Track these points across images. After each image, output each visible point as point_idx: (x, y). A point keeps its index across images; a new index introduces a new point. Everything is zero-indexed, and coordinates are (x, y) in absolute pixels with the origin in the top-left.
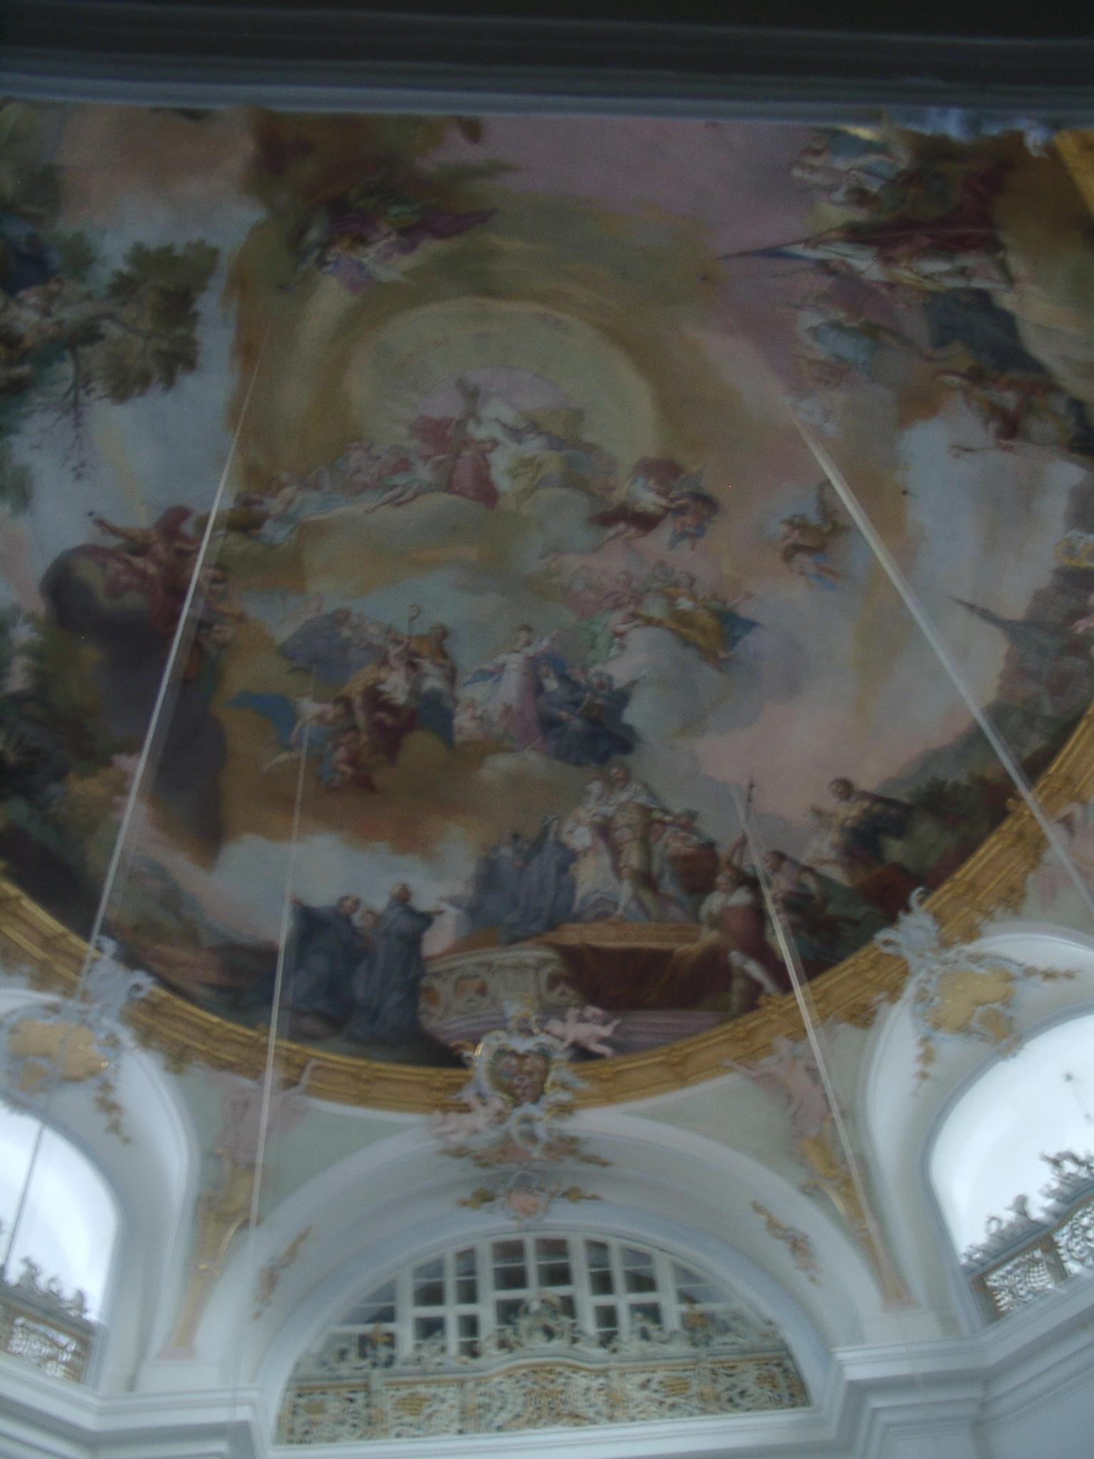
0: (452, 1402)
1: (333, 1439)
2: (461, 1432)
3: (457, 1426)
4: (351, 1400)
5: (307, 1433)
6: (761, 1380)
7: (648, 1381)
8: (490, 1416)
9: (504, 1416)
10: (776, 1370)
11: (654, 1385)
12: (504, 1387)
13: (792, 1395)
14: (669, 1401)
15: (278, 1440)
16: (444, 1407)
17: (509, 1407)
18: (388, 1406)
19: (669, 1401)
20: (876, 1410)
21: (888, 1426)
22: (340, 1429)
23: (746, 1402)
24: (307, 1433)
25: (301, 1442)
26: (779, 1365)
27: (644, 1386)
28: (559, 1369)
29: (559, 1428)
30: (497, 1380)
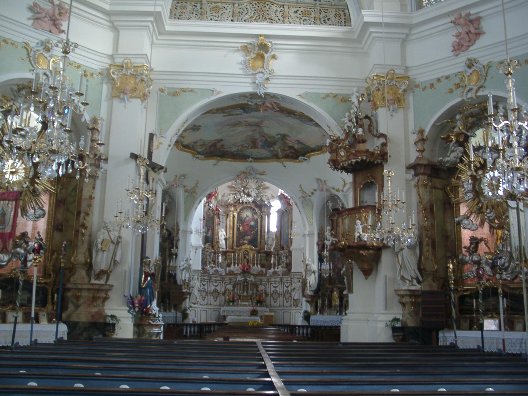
0: (230, 10)
1: (189, 19)
2: (232, 20)
3: (231, 18)
4: (196, 6)
5: (180, 16)
6: (336, 15)
7: (298, 10)
8: (242, 16)
9: (247, 16)
10: (342, 13)
11: (299, 12)
12: (247, 7)
13: (345, 22)
14: (303, 18)
15: (170, 18)
16: (228, 11)
17: (249, 14)
18: (208, 10)
19: (303, 18)
20: (371, 32)
21: (374, 37)
22: (191, 15)
23: (330, 22)
24: (180, 16)
25: (178, 19)
26: (343, 11)
27: (296, 12)
28: (267, 3)
29: (264, 23)
30: (246, 4)
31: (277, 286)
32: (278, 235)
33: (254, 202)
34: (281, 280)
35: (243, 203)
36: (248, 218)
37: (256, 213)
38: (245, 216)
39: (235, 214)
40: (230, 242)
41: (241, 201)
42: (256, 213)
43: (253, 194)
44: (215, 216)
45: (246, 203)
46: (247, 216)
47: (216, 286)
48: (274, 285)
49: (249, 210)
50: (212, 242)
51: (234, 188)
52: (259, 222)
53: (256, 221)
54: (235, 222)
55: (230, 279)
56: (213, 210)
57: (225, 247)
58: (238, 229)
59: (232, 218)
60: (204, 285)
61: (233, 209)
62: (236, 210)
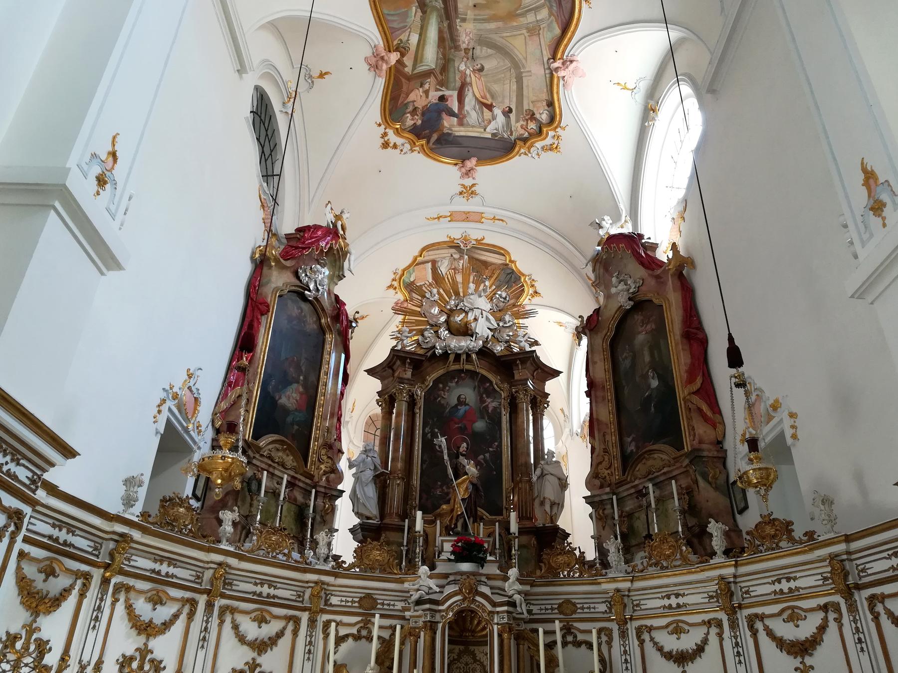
31: (700, 649)
32: (613, 418)
33: (484, 353)
34: (727, 595)
35: (445, 355)
36: (462, 409)
37: (492, 392)
38: (455, 402)
39: (420, 393)
40: (396, 492)
41: (439, 351)
42: (492, 392)
43: (482, 328)
44: (328, 337)
45: (458, 357)
46: (461, 402)
47: (262, 646)
48: (671, 643)
49: (468, 381)
50: (300, 444)
51: (419, 314)
52: (505, 419)
53: (495, 421)
54: (419, 422)
55: (368, 604)
56: (315, 304)
57: (373, 509)
58: (429, 446)
59: (404, 407)
60: (146, 629)
61: (408, 374)
62: (423, 381)
